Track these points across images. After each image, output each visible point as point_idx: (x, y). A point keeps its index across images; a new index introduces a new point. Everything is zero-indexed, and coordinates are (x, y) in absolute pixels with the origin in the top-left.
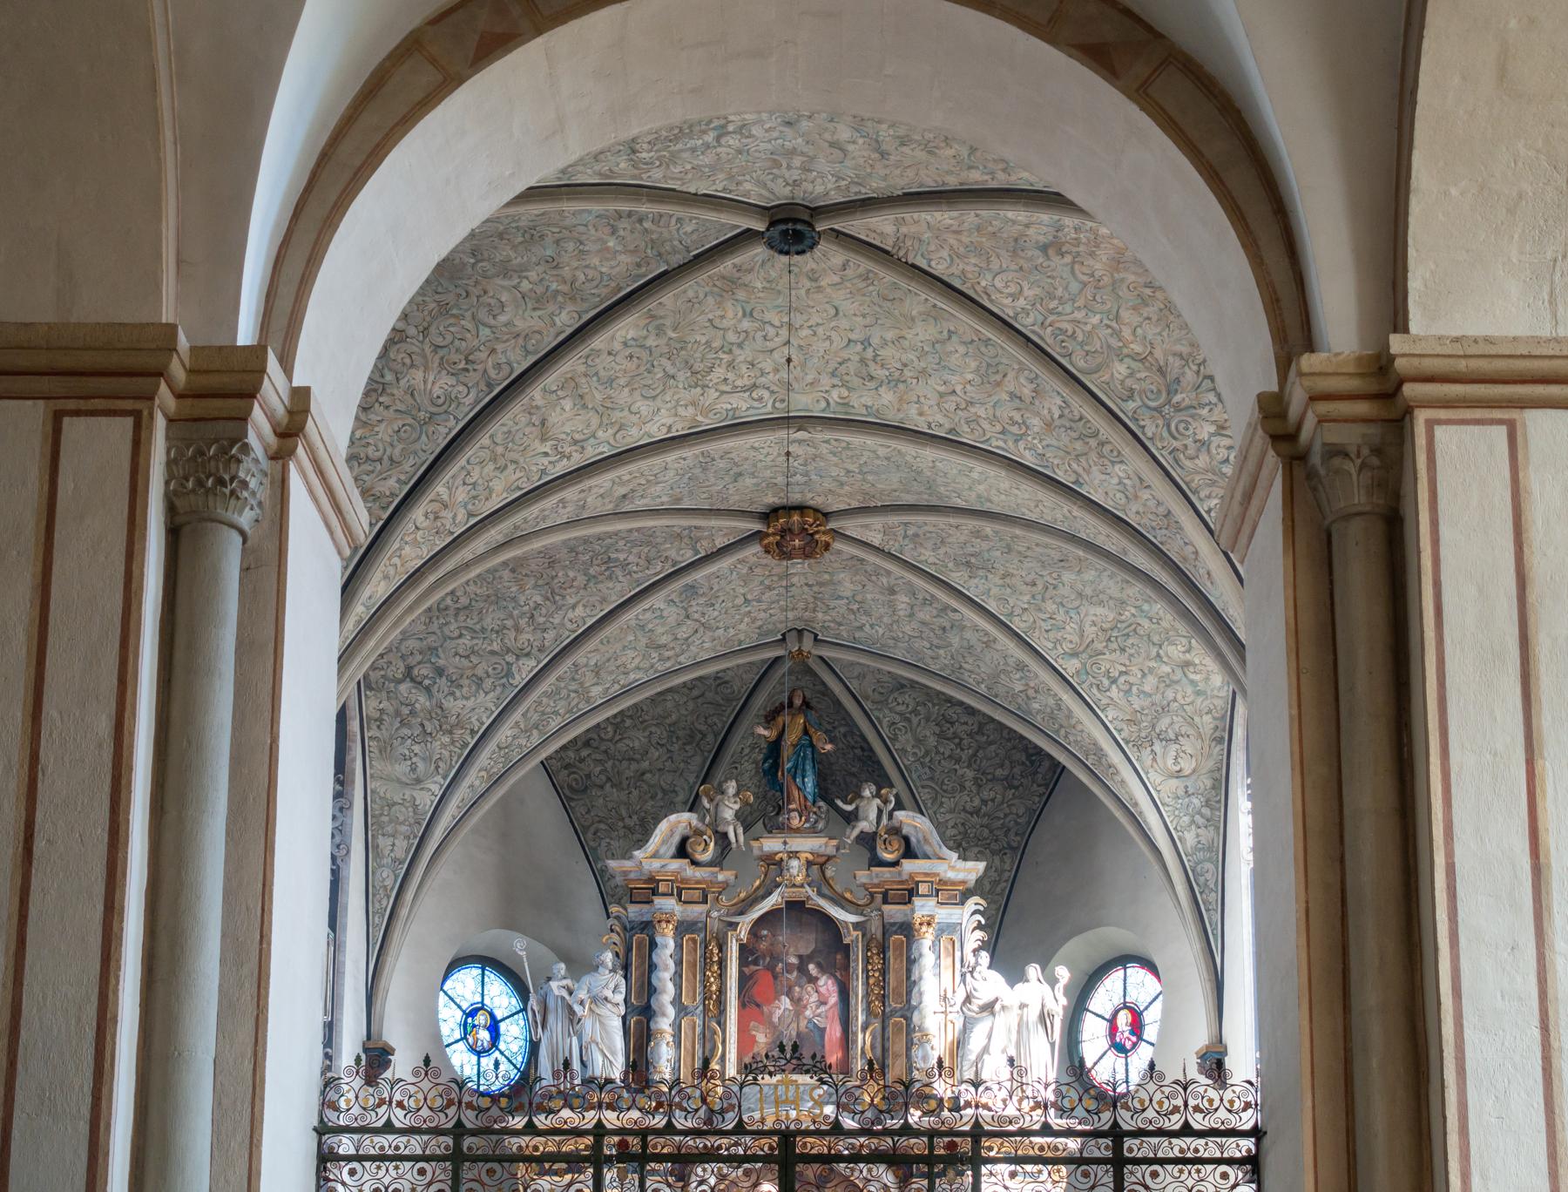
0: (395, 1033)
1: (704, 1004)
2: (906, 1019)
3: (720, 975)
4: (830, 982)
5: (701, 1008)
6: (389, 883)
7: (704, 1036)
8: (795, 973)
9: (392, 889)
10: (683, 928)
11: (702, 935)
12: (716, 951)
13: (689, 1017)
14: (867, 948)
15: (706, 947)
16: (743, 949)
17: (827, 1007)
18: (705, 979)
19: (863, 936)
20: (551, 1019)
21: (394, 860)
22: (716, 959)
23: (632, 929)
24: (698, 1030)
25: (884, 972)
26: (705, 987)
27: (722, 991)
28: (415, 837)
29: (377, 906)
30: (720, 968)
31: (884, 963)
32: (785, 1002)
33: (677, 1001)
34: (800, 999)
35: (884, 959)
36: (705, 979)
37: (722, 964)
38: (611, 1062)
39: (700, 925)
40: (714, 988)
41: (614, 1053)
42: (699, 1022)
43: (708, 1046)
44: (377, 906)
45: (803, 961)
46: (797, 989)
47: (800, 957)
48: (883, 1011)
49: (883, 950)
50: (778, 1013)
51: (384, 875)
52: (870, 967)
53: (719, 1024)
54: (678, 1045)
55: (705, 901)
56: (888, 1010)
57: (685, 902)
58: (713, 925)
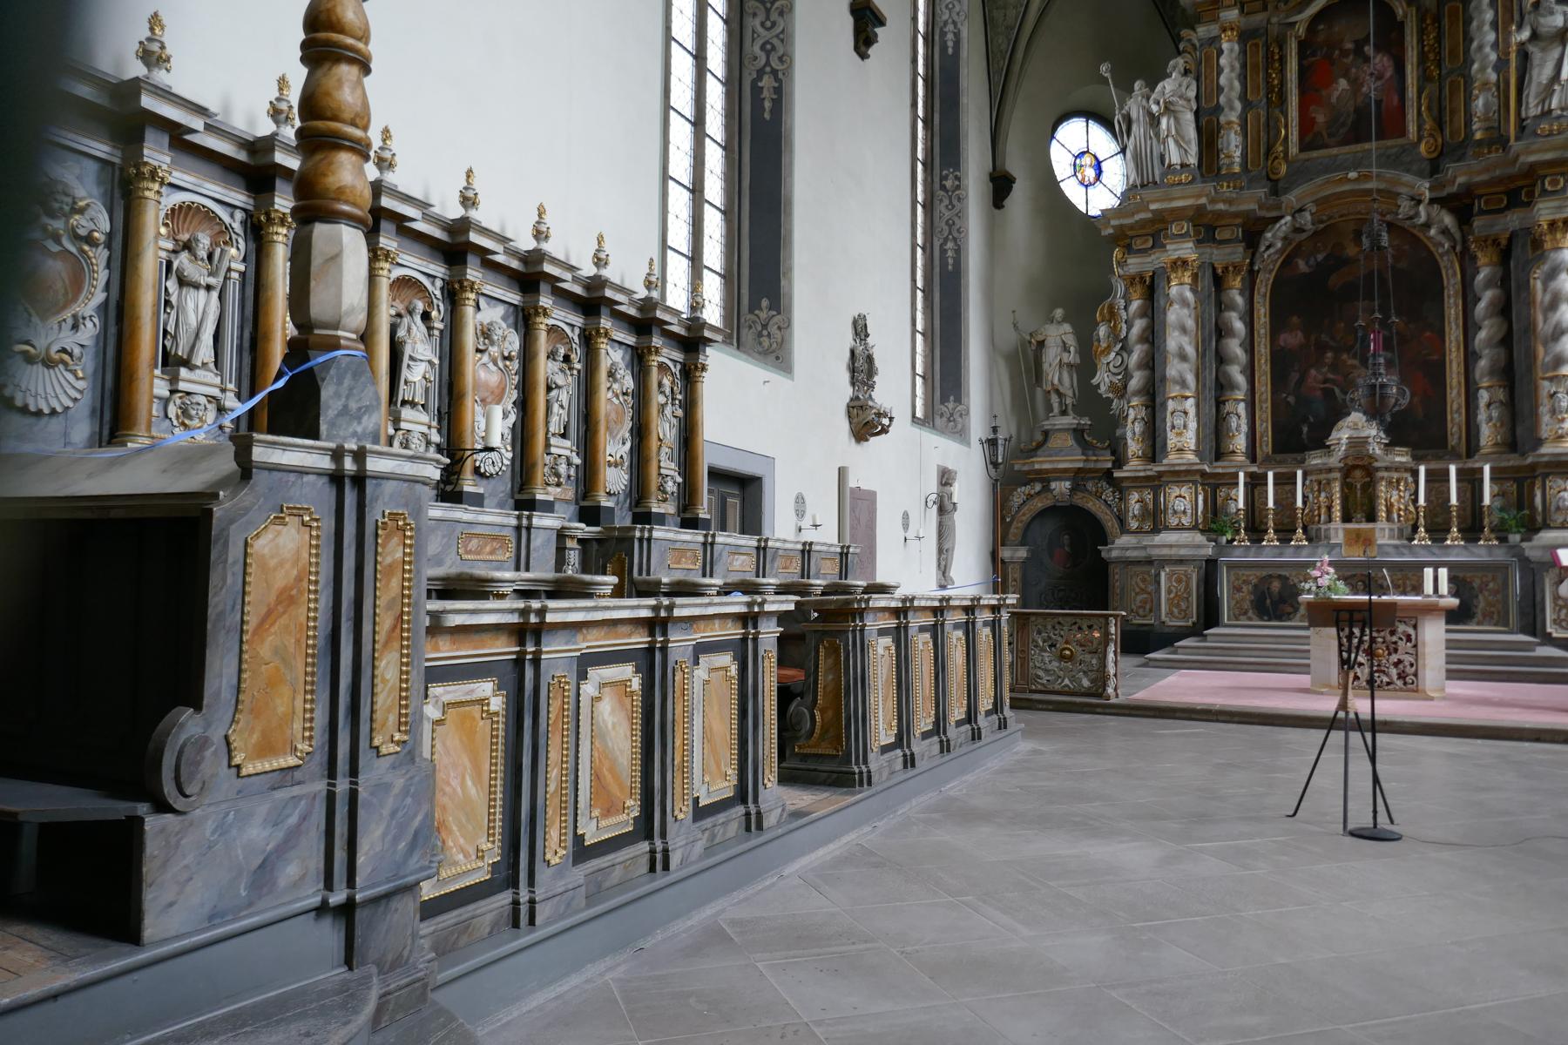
0: (1015, 165)
1: (1267, 98)
2: (1464, 76)
3: (1281, 70)
4: (1385, 59)
5: (1265, 100)
6: (1004, 47)
7: (1268, 125)
8: (1351, 57)
9: (1006, 52)
10: (1245, 37)
11: (1264, 38)
12: (1276, 51)
13: (1254, 110)
14: (1421, 19)
15: (1268, 49)
16: (1302, 46)
17: (1383, 81)
18: (1268, 75)
19: (1418, 10)
20: (1134, 128)
21: (1007, 28)
22: (1277, 57)
23: (1201, 45)
24: (1263, 120)
25: (1439, 39)
26: (1268, 83)
27: (1283, 83)
28: (1021, 6)
29: (996, 66)
30: (1281, 65)
31: (1439, 33)
32: (1343, 84)
33: (1243, 97)
34: (1356, 79)
35: (1439, 27)
36: (1268, 75)
37: (1282, 60)
38: (1186, 150)
39: (1262, 31)
40: (1276, 82)
41: (1188, 143)
42: (1263, 113)
43: (1272, 133)
44: (996, 66)
45: (1360, 45)
46: (1354, 70)
47: (1356, 42)
48: (1439, 75)
49: (1437, 19)
50: (1336, 94)
51: (1000, 41)
52: (1425, 37)
53: (1282, 112)
54: (1245, 136)
55: (1265, 9)
56: (1444, 72)
57: (1247, 14)
58: (1274, 30)
